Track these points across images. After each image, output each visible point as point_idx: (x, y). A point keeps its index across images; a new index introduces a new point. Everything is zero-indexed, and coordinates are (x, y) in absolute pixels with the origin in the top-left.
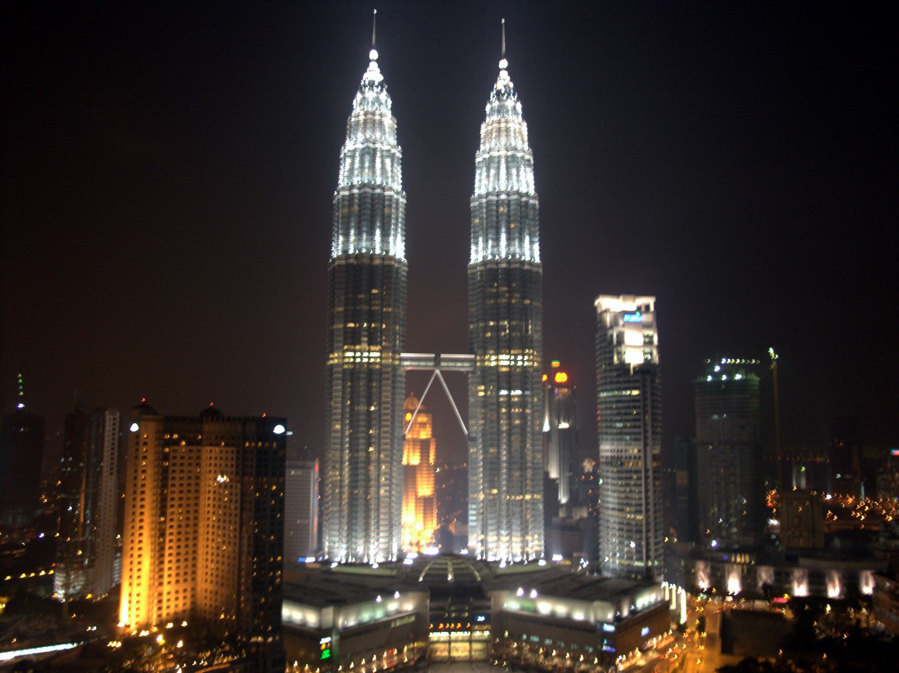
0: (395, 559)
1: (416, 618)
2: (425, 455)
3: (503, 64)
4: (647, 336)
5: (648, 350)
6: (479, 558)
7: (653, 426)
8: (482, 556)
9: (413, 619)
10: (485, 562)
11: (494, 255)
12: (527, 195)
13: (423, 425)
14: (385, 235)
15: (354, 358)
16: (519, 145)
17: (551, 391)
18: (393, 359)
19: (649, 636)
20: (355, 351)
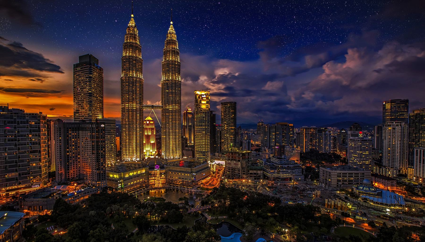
2: (152, 133)
4: (208, 101)
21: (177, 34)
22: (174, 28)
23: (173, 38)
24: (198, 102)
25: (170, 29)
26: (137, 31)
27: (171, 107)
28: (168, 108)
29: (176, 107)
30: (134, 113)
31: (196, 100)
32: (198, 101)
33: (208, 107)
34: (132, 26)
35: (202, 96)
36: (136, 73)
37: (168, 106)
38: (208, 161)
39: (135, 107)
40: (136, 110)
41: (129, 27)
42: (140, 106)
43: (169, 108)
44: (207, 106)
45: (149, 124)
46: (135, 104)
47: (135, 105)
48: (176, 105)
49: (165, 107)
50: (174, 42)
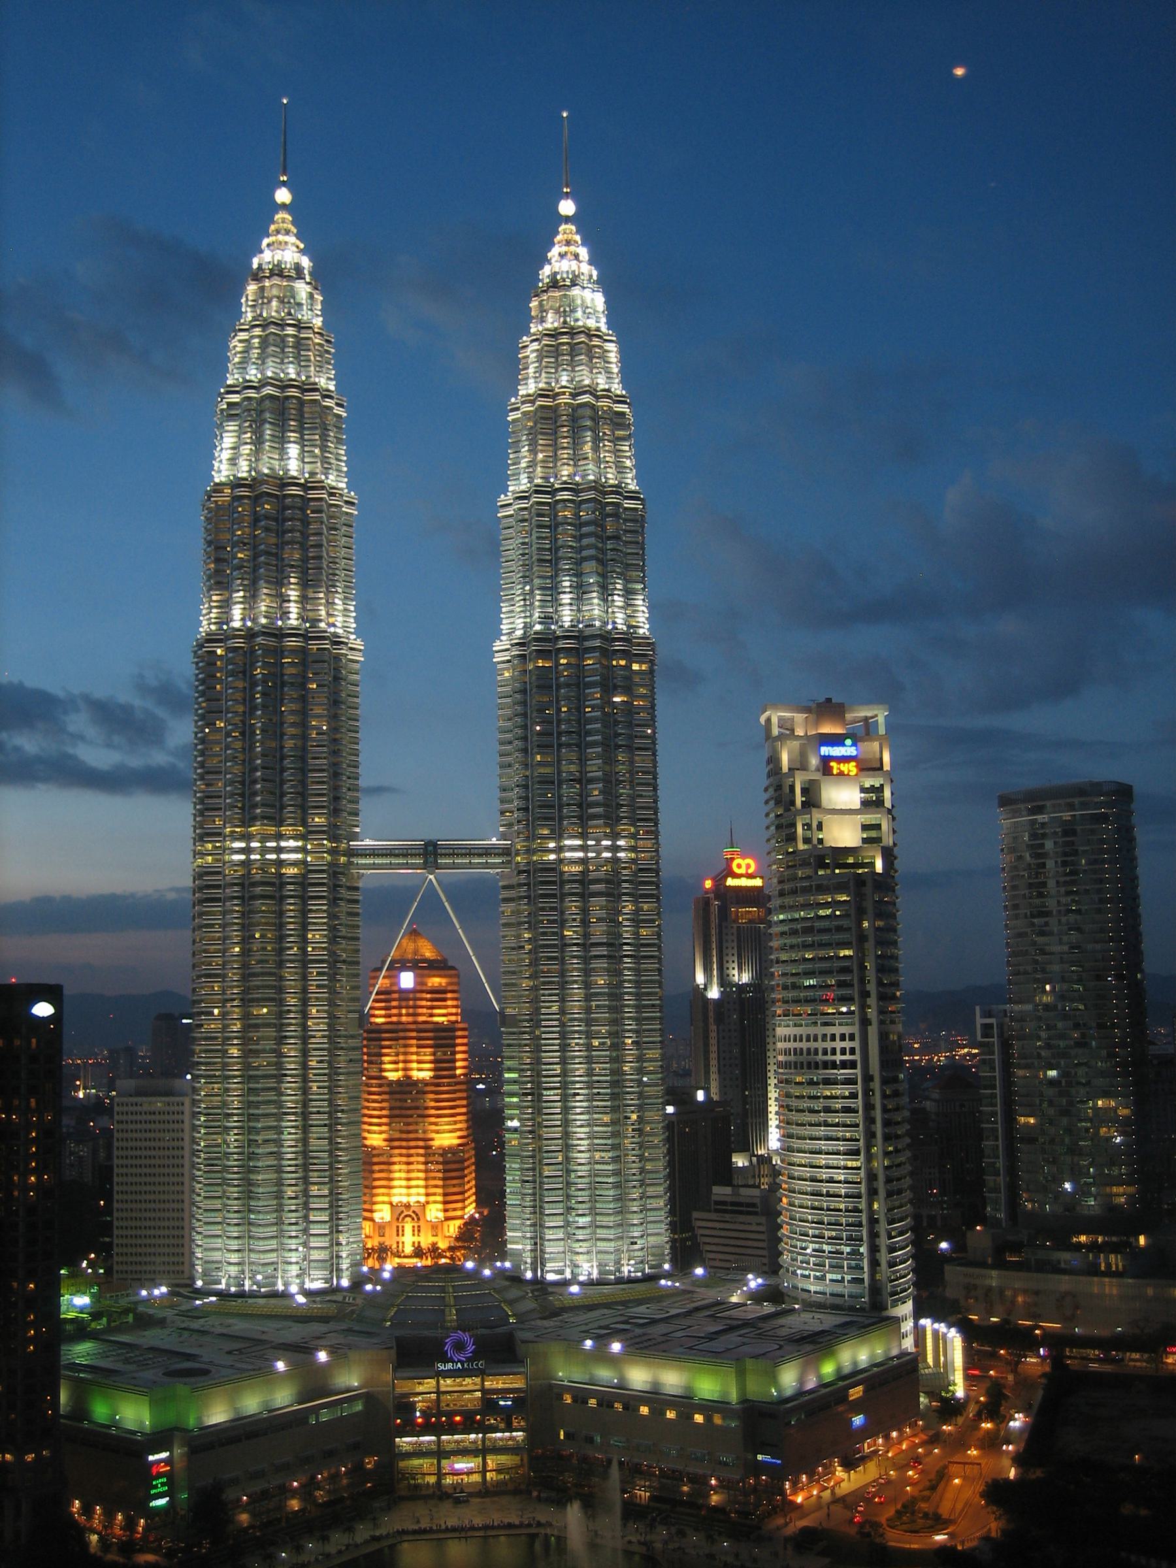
0: (345, 1283)
1: (366, 1405)
3: (567, 207)
4: (872, 789)
5: (870, 818)
6: (529, 1275)
7: (880, 983)
8: (535, 1271)
9: (359, 1407)
10: (539, 1284)
11: (546, 619)
12: (618, 490)
13: (439, 994)
14: (305, 584)
15: (247, 851)
16: (602, 382)
17: (724, 912)
18: (333, 852)
19: (867, 1432)
20: (247, 837)
21: (605, 283)
22: (584, 243)
23: (579, 314)
24: (793, 803)
25: (554, 253)
26: (311, 296)
27: (573, 849)
28: (552, 857)
29: (615, 849)
30: (291, 907)
31: (779, 787)
32: (792, 788)
33: (877, 840)
34: (278, 271)
35: (825, 751)
36: (304, 599)
37: (552, 845)
38: (895, 1304)
39: (294, 864)
40: (302, 882)
41: (257, 276)
42: (333, 852)
43: (561, 861)
44: (865, 828)
45: (413, 991)
46: (295, 838)
47: (292, 843)
48: (615, 836)
49: (529, 851)
50: (590, 348)
